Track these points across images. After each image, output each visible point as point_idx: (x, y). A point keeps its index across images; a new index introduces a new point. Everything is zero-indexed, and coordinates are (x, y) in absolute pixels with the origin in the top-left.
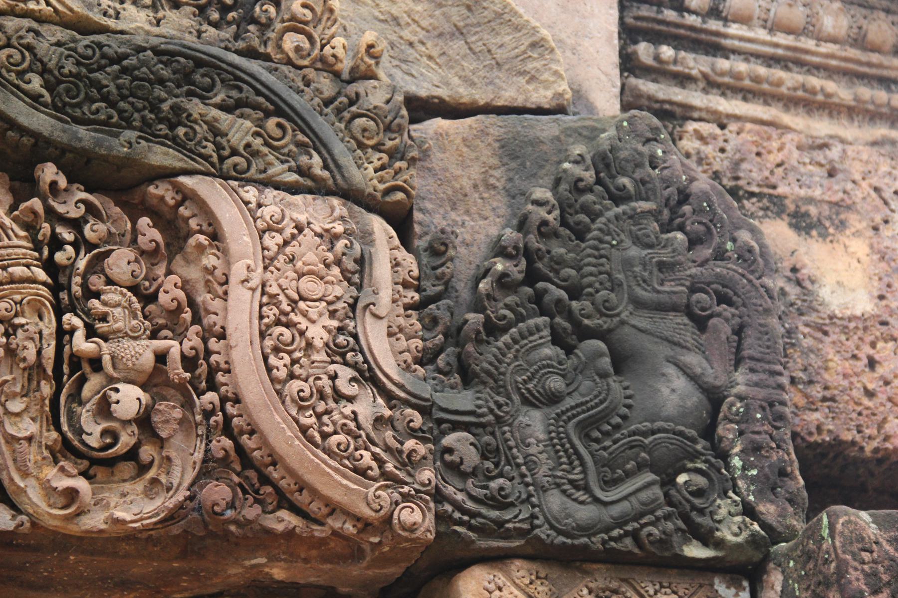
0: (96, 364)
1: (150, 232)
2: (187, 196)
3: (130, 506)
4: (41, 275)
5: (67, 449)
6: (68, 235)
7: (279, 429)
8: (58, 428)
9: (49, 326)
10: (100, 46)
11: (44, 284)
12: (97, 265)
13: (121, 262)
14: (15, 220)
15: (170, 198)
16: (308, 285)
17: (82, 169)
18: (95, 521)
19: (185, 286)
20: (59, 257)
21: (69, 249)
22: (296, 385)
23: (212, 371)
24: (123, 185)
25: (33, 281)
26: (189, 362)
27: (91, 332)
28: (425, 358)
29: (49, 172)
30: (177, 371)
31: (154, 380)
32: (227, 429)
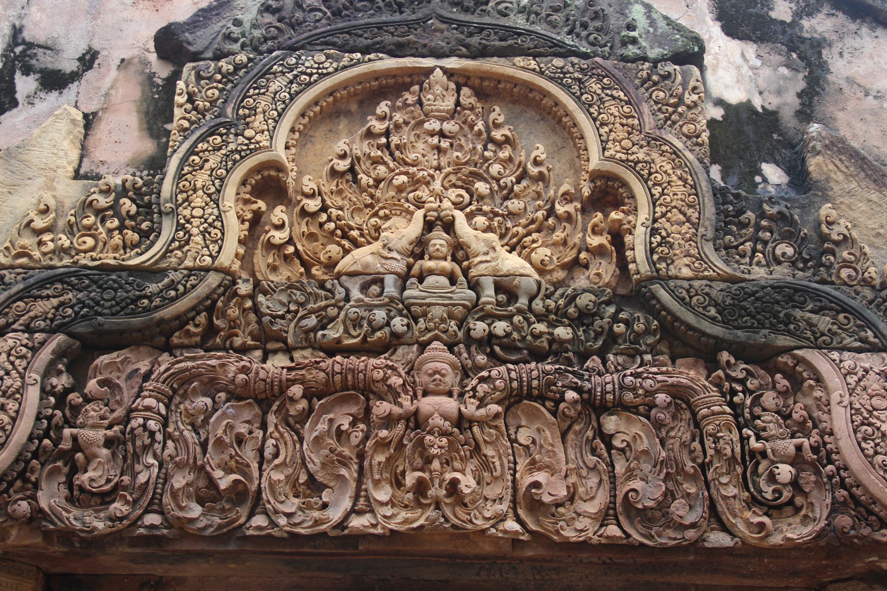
0: (763, 454)
1: (782, 382)
2: (800, 360)
3: (794, 531)
4: (728, 409)
5: (755, 502)
6: (739, 388)
8: (748, 490)
9: (735, 436)
10: (743, 288)
11: (730, 414)
12: (756, 401)
13: (769, 399)
14: (710, 382)
15: (790, 362)
17: (742, 352)
18: (776, 539)
19: (806, 408)
20: (736, 399)
21: (740, 394)
23: (829, 453)
24: (763, 358)
25: (724, 413)
26: (815, 449)
27: (758, 438)
29: (725, 356)
30: (809, 455)
31: (797, 460)
32: (843, 485)
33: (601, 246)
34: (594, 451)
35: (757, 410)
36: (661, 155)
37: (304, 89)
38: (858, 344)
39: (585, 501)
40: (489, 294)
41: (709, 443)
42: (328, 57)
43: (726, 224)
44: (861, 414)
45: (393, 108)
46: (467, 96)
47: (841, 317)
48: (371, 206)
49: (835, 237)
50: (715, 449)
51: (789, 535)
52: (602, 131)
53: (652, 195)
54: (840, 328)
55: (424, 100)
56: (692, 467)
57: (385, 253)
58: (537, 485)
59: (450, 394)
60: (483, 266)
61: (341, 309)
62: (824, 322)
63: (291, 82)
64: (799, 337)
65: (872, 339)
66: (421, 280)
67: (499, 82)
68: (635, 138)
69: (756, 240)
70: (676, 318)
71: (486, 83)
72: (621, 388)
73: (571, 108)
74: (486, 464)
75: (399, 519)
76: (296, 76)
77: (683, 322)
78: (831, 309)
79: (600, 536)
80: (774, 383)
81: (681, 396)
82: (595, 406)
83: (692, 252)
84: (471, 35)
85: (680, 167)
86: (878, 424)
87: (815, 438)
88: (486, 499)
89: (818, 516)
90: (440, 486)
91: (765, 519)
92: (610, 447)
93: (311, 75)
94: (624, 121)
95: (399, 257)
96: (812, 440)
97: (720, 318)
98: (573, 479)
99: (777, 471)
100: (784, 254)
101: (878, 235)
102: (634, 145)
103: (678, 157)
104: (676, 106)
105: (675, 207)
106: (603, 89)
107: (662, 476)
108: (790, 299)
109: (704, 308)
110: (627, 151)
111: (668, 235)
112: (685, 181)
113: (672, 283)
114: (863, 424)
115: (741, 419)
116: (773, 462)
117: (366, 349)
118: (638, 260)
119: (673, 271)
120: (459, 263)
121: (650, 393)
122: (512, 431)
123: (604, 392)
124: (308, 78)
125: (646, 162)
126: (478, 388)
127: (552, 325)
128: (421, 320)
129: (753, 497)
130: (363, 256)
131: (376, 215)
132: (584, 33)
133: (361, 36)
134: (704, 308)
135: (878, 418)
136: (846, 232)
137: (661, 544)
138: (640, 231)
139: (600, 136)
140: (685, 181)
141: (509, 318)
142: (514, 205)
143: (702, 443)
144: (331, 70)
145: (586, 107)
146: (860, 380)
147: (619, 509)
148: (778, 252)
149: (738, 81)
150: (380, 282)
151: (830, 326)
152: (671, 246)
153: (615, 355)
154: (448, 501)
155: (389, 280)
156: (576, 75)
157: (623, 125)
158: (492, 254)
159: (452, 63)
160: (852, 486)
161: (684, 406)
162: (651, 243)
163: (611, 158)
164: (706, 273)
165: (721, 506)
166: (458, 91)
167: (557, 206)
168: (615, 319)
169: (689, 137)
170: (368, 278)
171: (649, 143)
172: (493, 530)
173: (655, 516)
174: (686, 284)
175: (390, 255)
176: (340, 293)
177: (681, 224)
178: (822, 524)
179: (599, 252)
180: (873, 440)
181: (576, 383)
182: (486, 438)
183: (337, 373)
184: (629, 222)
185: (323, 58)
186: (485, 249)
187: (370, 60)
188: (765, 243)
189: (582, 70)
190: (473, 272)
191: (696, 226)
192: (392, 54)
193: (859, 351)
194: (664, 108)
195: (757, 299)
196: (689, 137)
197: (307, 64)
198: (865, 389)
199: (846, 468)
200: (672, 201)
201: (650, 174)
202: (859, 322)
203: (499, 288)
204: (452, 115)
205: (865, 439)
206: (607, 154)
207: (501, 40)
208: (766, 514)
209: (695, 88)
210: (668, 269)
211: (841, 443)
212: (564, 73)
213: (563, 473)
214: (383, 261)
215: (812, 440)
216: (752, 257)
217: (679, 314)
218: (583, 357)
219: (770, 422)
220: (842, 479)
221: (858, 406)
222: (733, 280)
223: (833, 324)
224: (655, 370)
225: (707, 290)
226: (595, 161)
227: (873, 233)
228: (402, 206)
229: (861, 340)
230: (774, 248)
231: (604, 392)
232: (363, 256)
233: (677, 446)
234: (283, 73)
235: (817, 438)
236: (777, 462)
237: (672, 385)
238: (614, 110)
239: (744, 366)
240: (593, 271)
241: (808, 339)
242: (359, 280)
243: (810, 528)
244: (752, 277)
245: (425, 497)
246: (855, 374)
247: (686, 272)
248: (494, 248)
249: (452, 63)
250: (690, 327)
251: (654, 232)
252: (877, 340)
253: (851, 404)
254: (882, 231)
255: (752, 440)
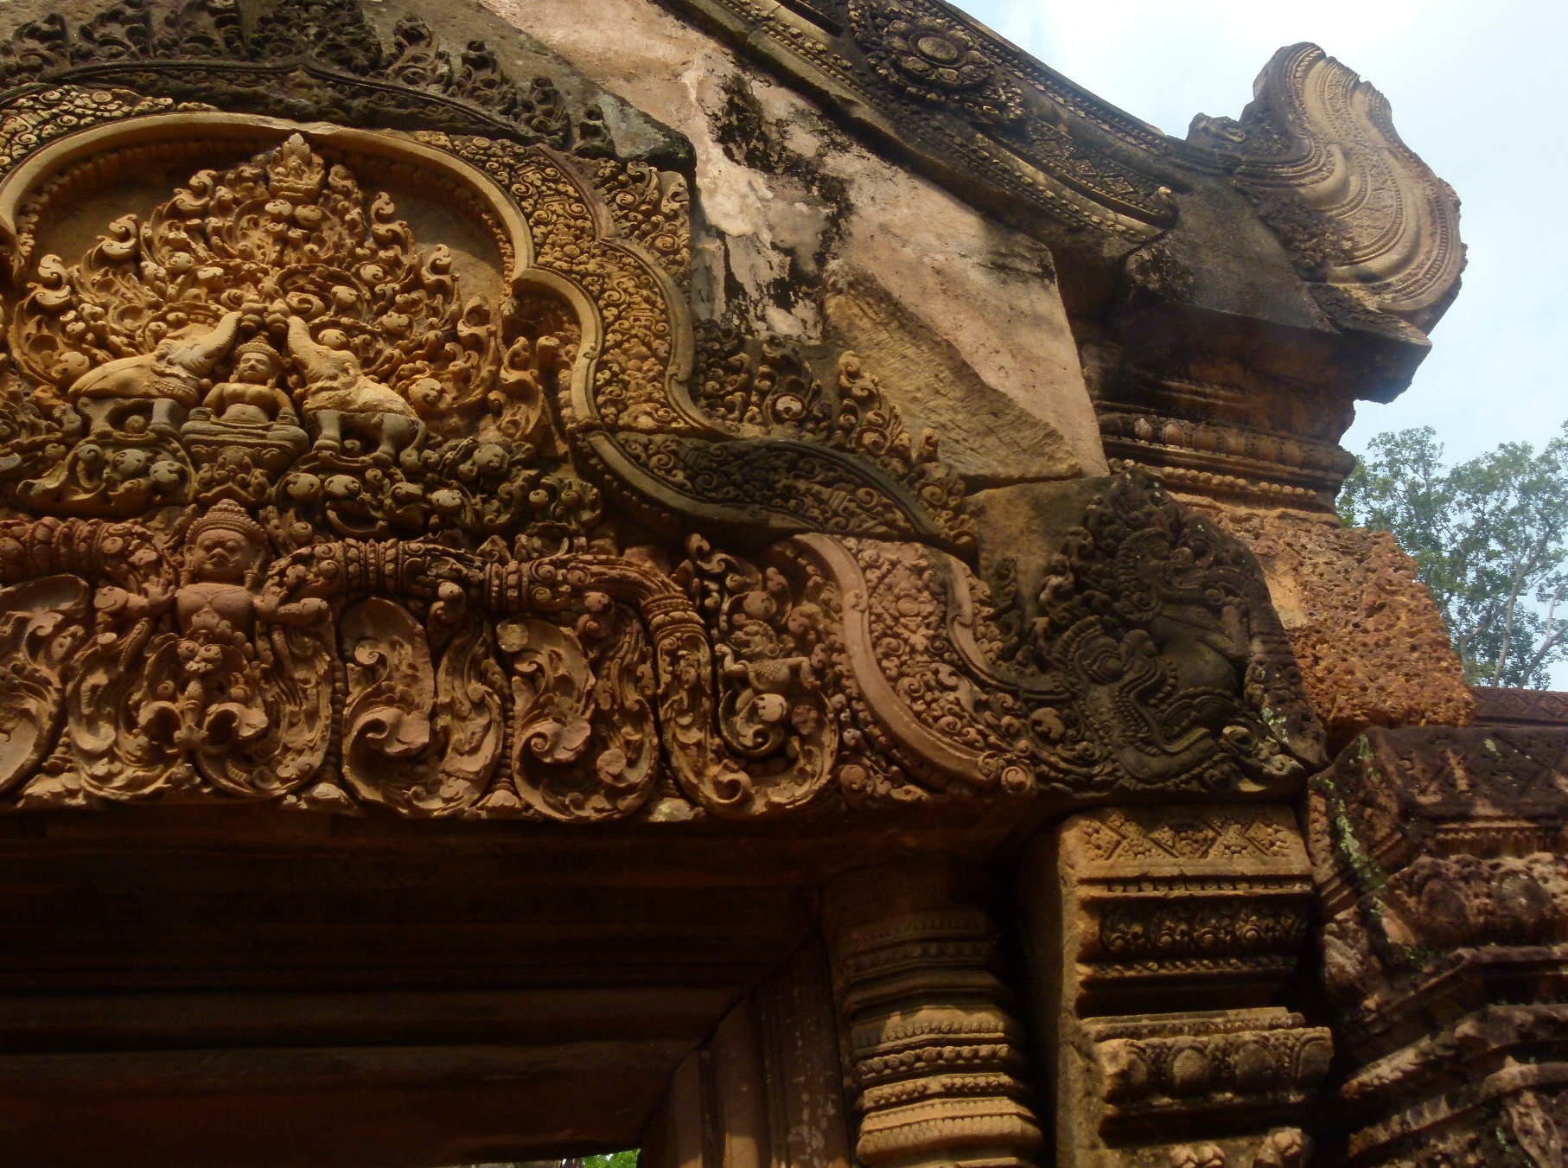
3: (787, 793)
4: (696, 617)
5: (728, 752)
7: (899, 716)
8: (720, 735)
9: (704, 654)
12: (737, 607)
13: (756, 600)
16: (904, 605)
17: (721, 536)
18: (759, 807)
20: (708, 602)
22: (906, 681)
26: (818, 672)
27: (737, 657)
28: (1006, 655)
29: (696, 541)
30: (809, 680)
31: (791, 688)
32: (855, 722)
33: (521, 384)
34: (482, 677)
35: (739, 618)
36: (621, 269)
37: (65, 134)
38: (883, 529)
39: (462, 755)
40: (329, 433)
41: (664, 663)
42: (116, 97)
43: (710, 366)
44: (884, 621)
45: (218, 181)
46: (338, 177)
47: (861, 492)
48: (155, 306)
49: (857, 392)
50: (672, 673)
51: (776, 799)
52: (536, 231)
53: (603, 319)
54: (859, 506)
55: (272, 175)
56: (637, 701)
57: (161, 366)
58: (377, 726)
59: (239, 581)
60: (325, 394)
61: (70, 447)
62: (838, 498)
63: (46, 122)
64: (804, 518)
65: (902, 523)
66: (220, 411)
67: (393, 163)
68: (585, 244)
69: (746, 388)
70: (625, 483)
71: (372, 163)
72: (531, 582)
73: (493, 199)
74: (294, 692)
75: (118, 782)
76: (55, 116)
77: (636, 491)
78: (849, 482)
79: (482, 808)
80: (766, 579)
81: (627, 600)
82: (483, 609)
83: (656, 395)
84: (354, 96)
85: (648, 286)
86: (906, 634)
87: (818, 655)
88: (286, 749)
89: (818, 770)
90: (199, 724)
91: (742, 777)
92: (509, 672)
93: (84, 116)
94: (572, 222)
95: (184, 374)
96: (815, 659)
97: (689, 485)
98: (443, 721)
99: (761, 703)
100: (788, 410)
101: (914, 400)
102: (582, 253)
103: (645, 272)
104: (648, 215)
105: (636, 336)
106: (544, 180)
107: (588, 714)
108: (792, 467)
109: (669, 472)
110: (571, 258)
111: (623, 371)
112: (653, 304)
113: (622, 436)
114: (884, 635)
115: (714, 632)
116: (758, 692)
117: (106, 509)
118: (575, 402)
119: (624, 419)
120: (289, 391)
121: (578, 591)
122: (347, 645)
123: (503, 587)
124: (75, 120)
125: (598, 276)
126: (289, 571)
127: (431, 487)
128: (206, 466)
129: (727, 744)
130: (117, 370)
131: (163, 318)
132: (525, 116)
133: (179, 78)
134: (669, 472)
135: (906, 627)
136: (871, 387)
137: (579, 818)
138: (581, 362)
139: (534, 237)
140: (653, 304)
141: (358, 473)
142: (393, 319)
143: (655, 667)
144: (118, 113)
145: (518, 200)
146: (884, 576)
147: (516, 765)
148: (780, 406)
149: (742, 211)
150: (146, 410)
151: (846, 503)
152: (626, 385)
153: (530, 536)
154: (213, 750)
155: (161, 407)
156: (506, 160)
157: (569, 227)
158: (343, 379)
159: (321, 128)
160: (867, 724)
161: (631, 613)
162: (595, 380)
163: (549, 265)
164: (674, 425)
165: (679, 760)
166: (327, 168)
167: (460, 326)
168: (533, 484)
169: (664, 254)
170: (127, 402)
171: (604, 254)
172: (291, 799)
173: (576, 776)
174: (643, 438)
175: (168, 371)
176: (73, 421)
177: (644, 359)
178: (823, 781)
179: (519, 393)
180: (899, 657)
181: (459, 571)
182: (296, 651)
183: (40, 542)
184: (567, 353)
185: (109, 97)
186: (333, 371)
187: (186, 109)
188: (763, 394)
189: (516, 155)
190: (310, 403)
191: (664, 362)
192: (224, 107)
193: (884, 538)
194: (632, 214)
195: (747, 463)
196: (664, 254)
197: (78, 102)
198: (890, 588)
199: (861, 697)
200: (632, 327)
201: (603, 291)
202: (885, 500)
203: (349, 428)
204: (311, 198)
205: (886, 656)
206: (541, 260)
207: (398, 106)
208: (745, 770)
209: (676, 194)
210: (617, 416)
211: (856, 663)
212: (489, 156)
213: (428, 708)
214: (156, 378)
215: (815, 659)
216: (743, 414)
217: (629, 478)
218: (477, 535)
219: (755, 633)
220: (854, 714)
221: (879, 610)
222: (711, 435)
223: (850, 500)
224: (589, 557)
225: (673, 447)
226: (521, 265)
227: (909, 396)
228: (207, 308)
229: (885, 523)
230: (775, 402)
231: (503, 587)
232: (117, 370)
233: (615, 671)
234: (34, 110)
235: (822, 656)
236: (762, 692)
237: (612, 580)
238: (556, 207)
239: (723, 556)
240: (507, 417)
241: (815, 519)
242: (109, 407)
243: (806, 788)
244: (740, 435)
245: (171, 744)
246: (879, 568)
247: (645, 422)
248: (346, 371)
249: (321, 128)
250: (645, 497)
251: (602, 365)
252: (908, 525)
253: (870, 607)
254: (919, 395)
255: (728, 661)
